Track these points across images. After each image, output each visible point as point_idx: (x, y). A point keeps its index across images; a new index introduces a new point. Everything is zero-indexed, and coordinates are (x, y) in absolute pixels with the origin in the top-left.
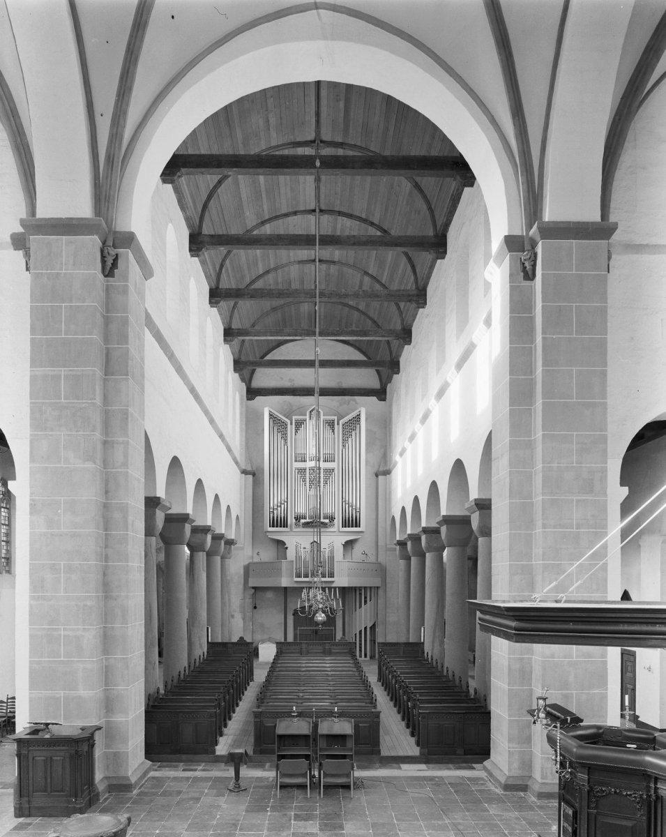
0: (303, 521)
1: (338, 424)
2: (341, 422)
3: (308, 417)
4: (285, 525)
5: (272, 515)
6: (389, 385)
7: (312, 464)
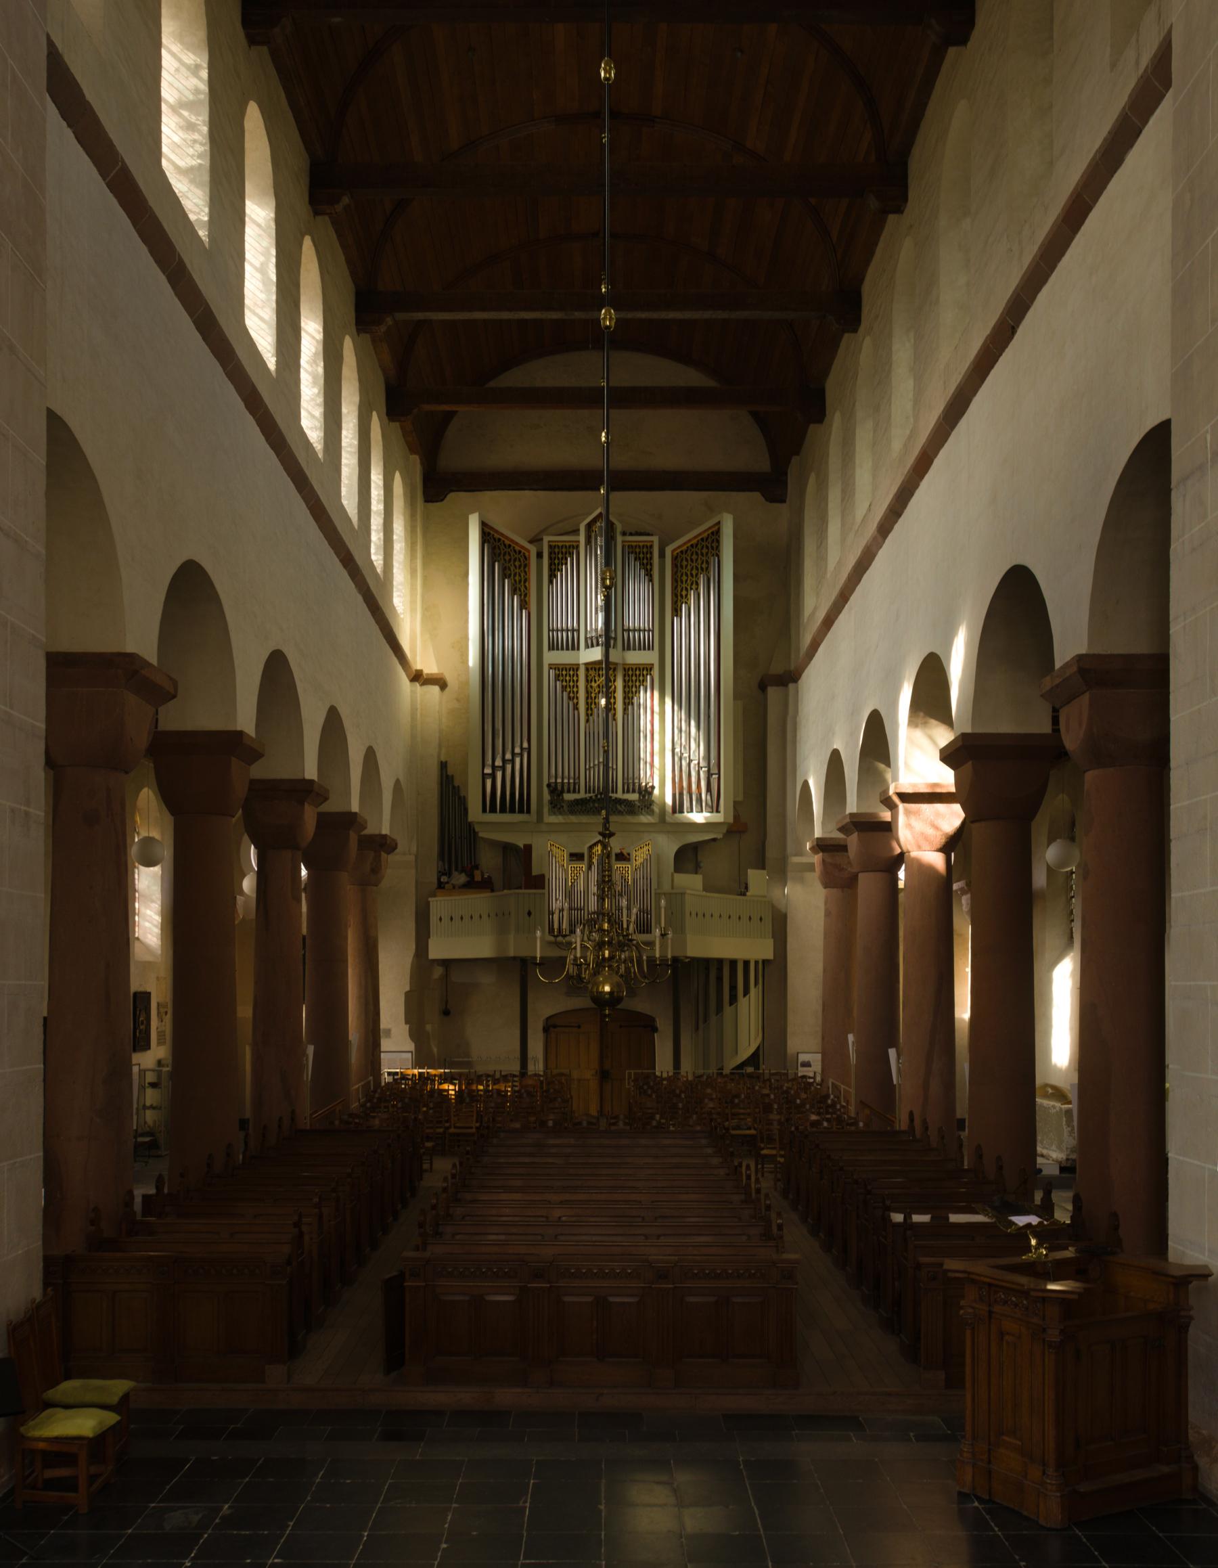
0: (568, 797)
1: (662, 555)
2: (668, 551)
3: (582, 539)
4: (522, 806)
5: (489, 782)
6: (795, 460)
7: (596, 654)
